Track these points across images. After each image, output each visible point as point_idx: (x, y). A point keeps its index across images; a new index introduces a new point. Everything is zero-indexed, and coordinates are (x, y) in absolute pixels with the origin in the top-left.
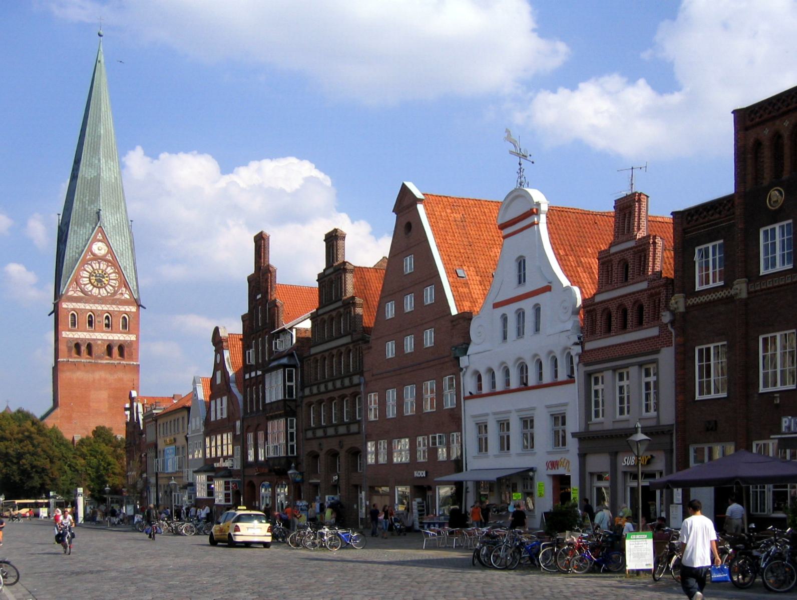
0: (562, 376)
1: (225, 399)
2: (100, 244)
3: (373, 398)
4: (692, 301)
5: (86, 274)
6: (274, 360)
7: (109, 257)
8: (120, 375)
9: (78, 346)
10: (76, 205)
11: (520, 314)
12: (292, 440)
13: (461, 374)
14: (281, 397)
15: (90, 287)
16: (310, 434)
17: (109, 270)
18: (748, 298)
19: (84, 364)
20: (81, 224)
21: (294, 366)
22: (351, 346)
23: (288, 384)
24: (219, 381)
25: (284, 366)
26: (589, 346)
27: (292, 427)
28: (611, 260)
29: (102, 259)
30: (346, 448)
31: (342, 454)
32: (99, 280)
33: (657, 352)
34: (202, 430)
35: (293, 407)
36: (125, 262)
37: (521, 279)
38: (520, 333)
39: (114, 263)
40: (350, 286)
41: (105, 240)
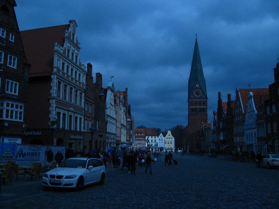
3: (235, 128)
5: (195, 92)
9: (193, 109)
26: (258, 122)
29: (198, 88)
38: (251, 119)
39: (201, 89)
41: (199, 83)
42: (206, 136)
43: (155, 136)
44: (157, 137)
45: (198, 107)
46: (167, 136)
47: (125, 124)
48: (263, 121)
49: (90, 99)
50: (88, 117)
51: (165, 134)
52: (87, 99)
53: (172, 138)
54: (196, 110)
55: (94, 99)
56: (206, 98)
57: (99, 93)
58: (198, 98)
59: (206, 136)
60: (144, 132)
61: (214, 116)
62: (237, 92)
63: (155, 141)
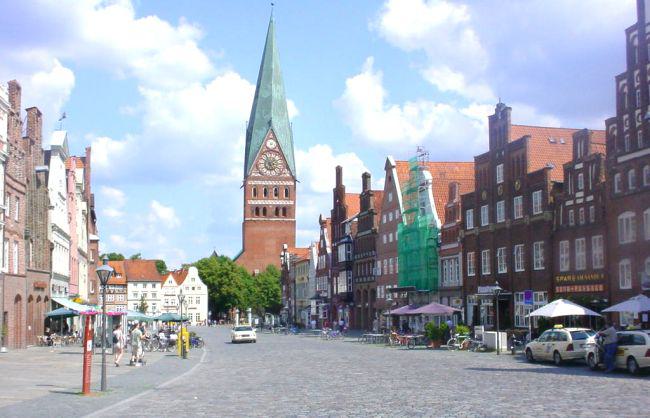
2: (271, 141)
3: (379, 263)
7: (277, 150)
8: (284, 228)
9: (257, 209)
10: (257, 116)
15: (265, 170)
17: (277, 158)
19: (261, 222)
20: (260, 128)
25: (345, 243)
31: (369, 291)
32: (270, 166)
36: (286, 152)
39: (281, 153)
40: (372, 201)
42: (294, 282)
43: (154, 282)
44: (158, 285)
45: (270, 202)
46: (187, 281)
47: (85, 250)
48: (455, 245)
49: (16, 181)
50: (12, 233)
51: (180, 276)
52: (9, 180)
53: (199, 288)
54: (265, 210)
55: (25, 182)
56: (294, 179)
57: (36, 164)
58: (270, 178)
59: (297, 282)
60: (123, 271)
61: (322, 228)
62: (388, 167)
63: (154, 295)
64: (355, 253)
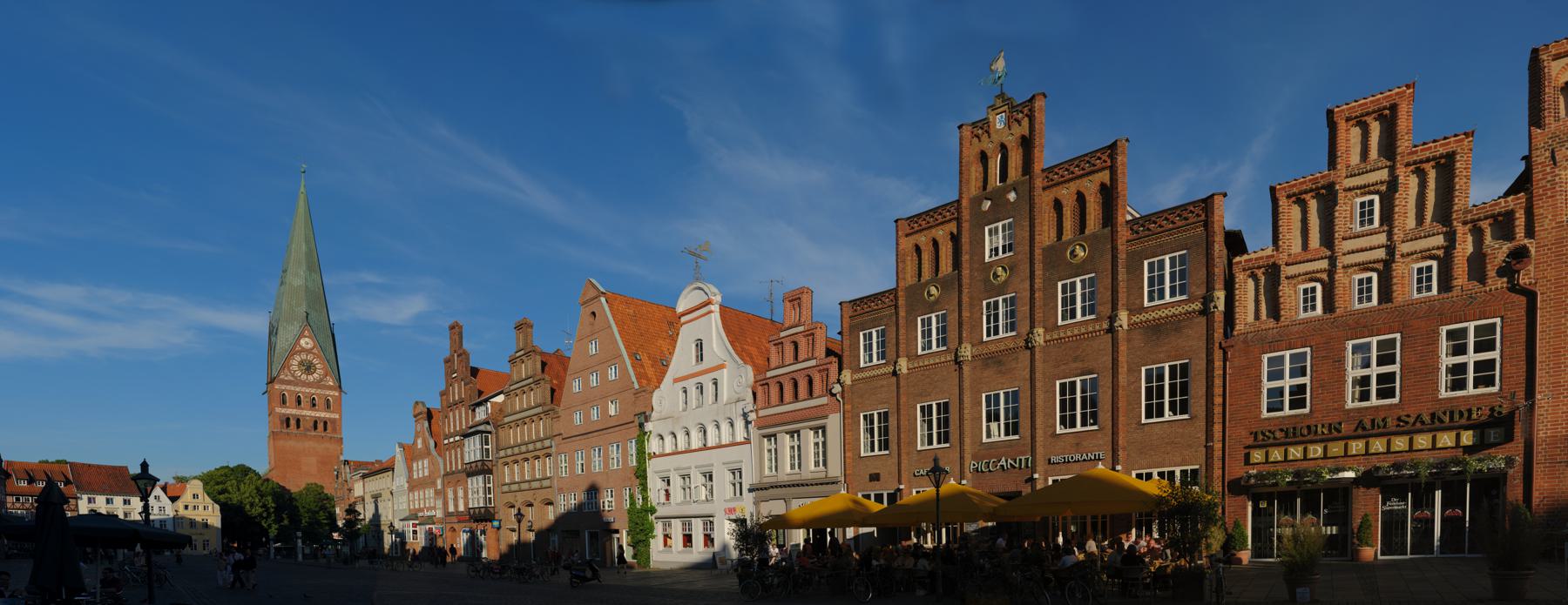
0: (740, 435)
1: (426, 462)
4: (856, 376)
6: (471, 428)
11: (701, 388)
12: (490, 493)
13: (646, 437)
14: (478, 457)
16: (506, 488)
18: (908, 374)
21: (490, 433)
22: (542, 415)
23: (485, 447)
24: (420, 446)
26: (762, 413)
27: (489, 483)
28: (782, 343)
30: (539, 500)
33: (826, 417)
34: (406, 485)
35: (490, 467)
37: (700, 358)
64: (498, 450)
